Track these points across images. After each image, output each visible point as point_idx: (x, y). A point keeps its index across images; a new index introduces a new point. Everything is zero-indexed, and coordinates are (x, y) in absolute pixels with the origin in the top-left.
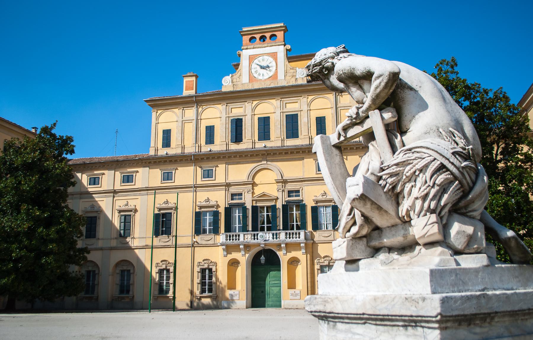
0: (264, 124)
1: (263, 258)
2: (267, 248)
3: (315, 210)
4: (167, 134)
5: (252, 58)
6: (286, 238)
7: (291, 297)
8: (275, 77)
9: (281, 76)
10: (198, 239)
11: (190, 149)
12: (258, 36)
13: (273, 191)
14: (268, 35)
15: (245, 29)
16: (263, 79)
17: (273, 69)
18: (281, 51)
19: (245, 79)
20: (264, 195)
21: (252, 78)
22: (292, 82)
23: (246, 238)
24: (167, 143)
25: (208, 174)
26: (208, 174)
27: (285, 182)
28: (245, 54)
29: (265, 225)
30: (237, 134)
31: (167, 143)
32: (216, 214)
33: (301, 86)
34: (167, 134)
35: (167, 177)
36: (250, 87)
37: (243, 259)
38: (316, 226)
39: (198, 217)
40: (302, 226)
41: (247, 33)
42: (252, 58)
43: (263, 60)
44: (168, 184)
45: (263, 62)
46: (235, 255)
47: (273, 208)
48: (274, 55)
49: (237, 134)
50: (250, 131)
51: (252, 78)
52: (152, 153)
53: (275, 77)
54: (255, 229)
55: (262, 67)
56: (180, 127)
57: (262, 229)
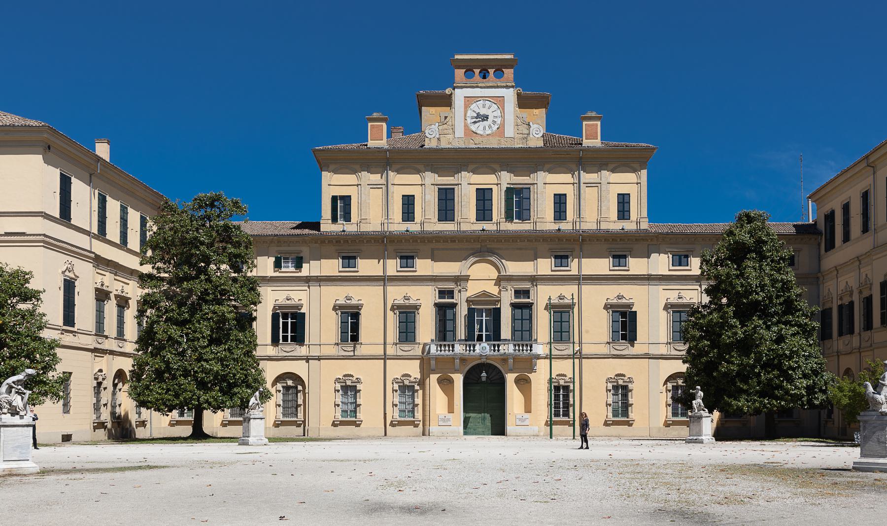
0: (484, 197)
1: (484, 374)
2: (488, 361)
6: (515, 350)
7: (519, 423)
9: (510, 131)
13: (494, 290)
15: (457, 57)
17: (499, 121)
18: (510, 95)
19: (460, 132)
20: (485, 294)
27: (510, 279)
28: (459, 95)
29: (484, 333)
30: (446, 209)
33: (536, 150)
41: (460, 64)
43: (484, 106)
47: (496, 313)
48: (500, 101)
49: (446, 209)
54: (471, 337)
55: (485, 118)
56: (374, 202)
57: (480, 339)
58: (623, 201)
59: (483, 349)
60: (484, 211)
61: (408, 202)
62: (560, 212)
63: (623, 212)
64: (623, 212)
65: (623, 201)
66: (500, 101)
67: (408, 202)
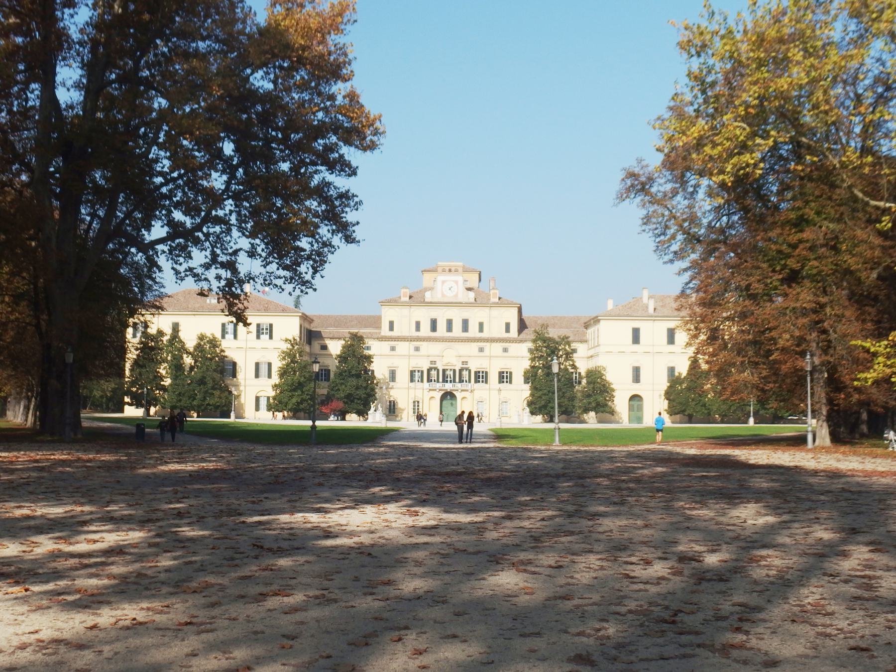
3: (476, 372)
4: (391, 324)
5: (443, 282)
8: (456, 296)
10: (412, 384)
11: (406, 333)
12: (447, 269)
14: (453, 269)
16: (449, 296)
21: (443, 295)
22: (467, 301)
23: (439, 385)
24: (391, 328)
25: (417, 349)
26: (417, 349)
30: (434, 328)
31: (391, 328)
32: (422, 372)
34: (391, 324)
35: (393, 349)
36: (442, 300)
37: (438, 395)
38: (476, 382)
39: (412, 373)
40: (470, 381)
42: (443, 282)
44: (393, 353)
45: (449, 286)
46: (433, 394)
48: (457, 282)
49: (434, 328)
50: (442, 326)
51: (443, 295)
52: (383, 334)
53: (456, 296)
58: (508, 326)
59: (448, 386)
60: (449, 327)
61: (418, 324)
62: (481, 329)
63: (508, 330)
64: (508, 330)
65: (508, 326)
66: (457, 282)
67: (418, 324)
